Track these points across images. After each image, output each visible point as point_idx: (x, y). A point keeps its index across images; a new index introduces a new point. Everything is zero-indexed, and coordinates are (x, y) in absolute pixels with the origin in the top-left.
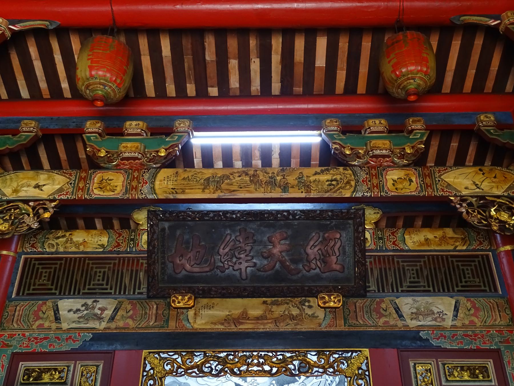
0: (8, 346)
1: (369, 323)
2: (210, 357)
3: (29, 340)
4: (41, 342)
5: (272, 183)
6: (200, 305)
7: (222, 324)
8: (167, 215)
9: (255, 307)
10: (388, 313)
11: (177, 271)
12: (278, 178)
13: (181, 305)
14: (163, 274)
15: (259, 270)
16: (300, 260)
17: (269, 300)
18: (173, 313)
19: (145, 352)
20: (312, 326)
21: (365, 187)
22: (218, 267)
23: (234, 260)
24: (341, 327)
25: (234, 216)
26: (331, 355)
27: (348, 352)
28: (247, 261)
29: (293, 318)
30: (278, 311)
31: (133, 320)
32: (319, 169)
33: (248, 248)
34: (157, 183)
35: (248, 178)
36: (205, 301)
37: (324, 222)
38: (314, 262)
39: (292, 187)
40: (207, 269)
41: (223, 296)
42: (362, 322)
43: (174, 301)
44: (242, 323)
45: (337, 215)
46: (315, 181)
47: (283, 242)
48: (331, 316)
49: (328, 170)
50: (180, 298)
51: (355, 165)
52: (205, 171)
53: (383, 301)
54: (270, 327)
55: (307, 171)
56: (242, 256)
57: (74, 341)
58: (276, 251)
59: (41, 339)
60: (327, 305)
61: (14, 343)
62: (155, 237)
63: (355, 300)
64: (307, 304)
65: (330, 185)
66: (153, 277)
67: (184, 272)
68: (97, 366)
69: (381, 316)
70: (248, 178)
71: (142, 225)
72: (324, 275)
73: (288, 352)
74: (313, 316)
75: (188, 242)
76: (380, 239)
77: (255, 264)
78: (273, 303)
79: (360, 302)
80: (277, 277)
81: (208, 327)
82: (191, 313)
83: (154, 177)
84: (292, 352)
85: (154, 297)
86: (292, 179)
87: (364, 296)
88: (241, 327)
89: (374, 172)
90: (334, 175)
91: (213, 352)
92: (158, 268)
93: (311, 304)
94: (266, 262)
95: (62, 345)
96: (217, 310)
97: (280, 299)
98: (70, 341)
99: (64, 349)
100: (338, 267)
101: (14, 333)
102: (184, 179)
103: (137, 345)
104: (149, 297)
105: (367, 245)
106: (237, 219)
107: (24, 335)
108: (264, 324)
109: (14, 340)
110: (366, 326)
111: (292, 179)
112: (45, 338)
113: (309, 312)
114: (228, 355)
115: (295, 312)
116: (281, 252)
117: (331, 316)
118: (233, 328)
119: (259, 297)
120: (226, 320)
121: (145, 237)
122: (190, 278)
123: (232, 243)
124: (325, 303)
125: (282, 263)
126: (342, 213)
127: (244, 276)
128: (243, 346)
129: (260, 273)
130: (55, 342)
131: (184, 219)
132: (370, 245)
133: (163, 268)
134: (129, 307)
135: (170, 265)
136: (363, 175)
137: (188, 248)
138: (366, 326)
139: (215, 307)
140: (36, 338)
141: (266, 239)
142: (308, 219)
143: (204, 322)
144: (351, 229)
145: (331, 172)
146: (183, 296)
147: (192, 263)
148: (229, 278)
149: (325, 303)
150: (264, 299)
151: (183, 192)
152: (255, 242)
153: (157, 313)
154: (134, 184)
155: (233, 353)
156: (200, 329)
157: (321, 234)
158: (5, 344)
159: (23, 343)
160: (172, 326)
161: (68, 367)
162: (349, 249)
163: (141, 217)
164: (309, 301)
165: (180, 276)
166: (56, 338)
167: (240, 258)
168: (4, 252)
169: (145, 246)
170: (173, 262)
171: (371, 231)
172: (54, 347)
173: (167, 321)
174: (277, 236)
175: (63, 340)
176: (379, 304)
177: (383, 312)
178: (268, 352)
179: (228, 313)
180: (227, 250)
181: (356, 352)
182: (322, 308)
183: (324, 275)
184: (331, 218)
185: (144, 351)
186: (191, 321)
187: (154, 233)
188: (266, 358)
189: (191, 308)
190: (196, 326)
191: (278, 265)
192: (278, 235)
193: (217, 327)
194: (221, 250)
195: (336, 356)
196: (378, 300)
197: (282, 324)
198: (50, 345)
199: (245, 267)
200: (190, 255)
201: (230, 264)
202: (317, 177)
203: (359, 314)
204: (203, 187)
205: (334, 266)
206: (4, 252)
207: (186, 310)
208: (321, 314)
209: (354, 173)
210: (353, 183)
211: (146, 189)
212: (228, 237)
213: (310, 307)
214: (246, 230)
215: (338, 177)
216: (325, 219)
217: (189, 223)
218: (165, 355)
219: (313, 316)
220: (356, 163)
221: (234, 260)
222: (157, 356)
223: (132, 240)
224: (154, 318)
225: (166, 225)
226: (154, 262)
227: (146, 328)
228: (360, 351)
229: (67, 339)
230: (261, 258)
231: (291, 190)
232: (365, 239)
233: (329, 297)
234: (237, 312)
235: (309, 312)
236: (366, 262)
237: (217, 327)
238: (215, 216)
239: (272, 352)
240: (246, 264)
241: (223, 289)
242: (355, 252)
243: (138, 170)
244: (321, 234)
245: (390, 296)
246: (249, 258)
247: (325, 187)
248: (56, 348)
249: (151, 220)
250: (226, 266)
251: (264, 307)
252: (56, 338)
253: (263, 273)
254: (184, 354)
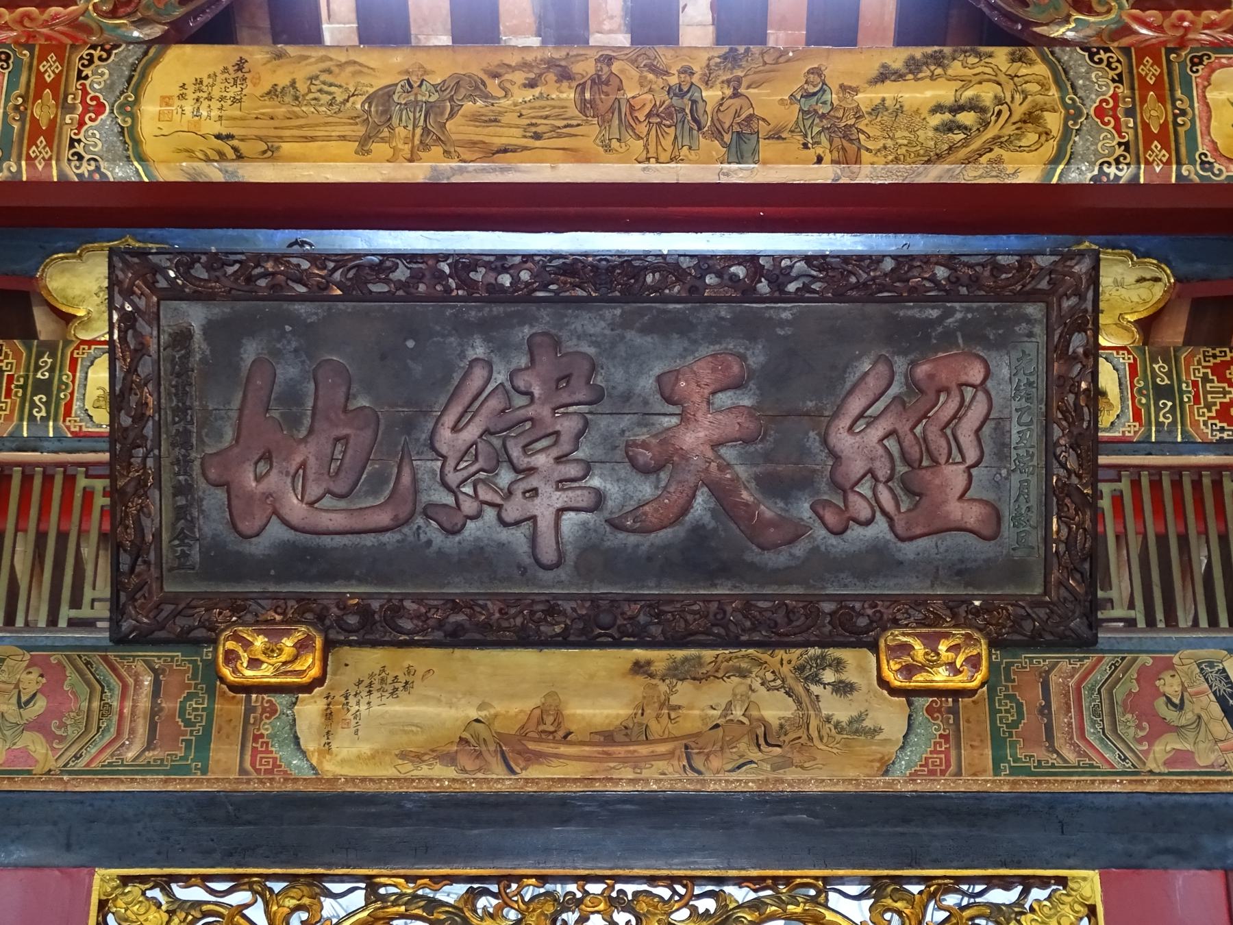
1: (1102, 760)
2: (395, 903)
5: (680, 116)
6: (347, 678)
7: (450, 759)
8: (200, 272)
9: (595, 687)
10: (1188, 717)
11: (246, 526)
12: (711, 95)
13: (265, 674)
14: (181, 536)
15: (615, 524)
16: (805, 482)
17: (660, 657)
18: (230, 709)
19: (103, 879)
20: (852, 773)
21: (1107, 141)
22: (429, 512)
23: (505, 477)
24: (978, 774)
25: (506, 280)
26: (932, 896)
27: (1006, 883)
28: (562, 484)
29: (765, 736)
30: (700, 704)
31: (50, 737)
32: (897, 58)
33: (568, 426)
34: (149, 109)
35: (568, 95)
36: (370, 659)
37: (911, 311)
38: (865, 489)
39: (776, 136)
40: (384, 518)
41: (455, 639)
42: (1071, 757)
43: (231, 657)
44: (538, 757)
45: (975, 281)
46: (876, 110)
47: (724, 399)
48: (937, 728)
49: (938, 60)
50: (260, 642)
51: (1064, 42)
52: (372, 58)
53: (1170, 666)
54: (662, 776)
55: (841, 66)
56: (541, 460)
58: (693, 439)
60: (919, 680)
62: (145, 368)
63: (1042, 660)
64: (829, 676)
65: (949, 128)
66: (138, 551)
67: (276, 531)
69: (1161, 728)
70: (568, 95)
71: (86, 322)
72: (909, 550)
73: (740, 882)
74: (857, 729)
75: (292, 397)
76: (1163, 392)
77: (599, 499)
78: (676, 672)
79: (1065, 669)
80: (699, 555)
81: (388, 774)
82: (310, 709)
83: (136, 79)
84: (757, 883)
85: (144, 639)
86: (772, 101)
87: (1087, 643)
88: (535, 772)
89: (1149, 71)
90: (966, 83)
91: (408, 879)
92: (159, 510)
93: (850, 676)
94: (645, 489)
96: (425, 699)
97: (708, 654)
100: (972, 514)
102: (273, 93)
103: (68, 847)
104: (120, 640)
105: (1105, 419)
106: (521, 296)
108: (636, 762)
110: (1092, 771)
111: (772, 101)
113: (840, 710)
114: (472, 895)
115: (776, 709)
116: (716, 445)
117: (937, 728)
118: (497, 780)
119: (617, 644)
120: (466, 744)
121: (99, 376)
122: (303, 557)
123: (495, 404)
124: (909, 671)
125: (722, 493)
126: (997, 269)
127: (548, 553)
128: (546, 852)
129: (621, 535)
131: (277, 293)
132: (1115, 419)
133: (181, 513)
134: (32, 681)
135: (214, 499)
136: (1099, 86)
137: (293, 421)
138: (1092, 771)
139: (419, 688)
141: (647, 384)
142: (839, 297)
143: (366, 748)
144: (1035, 346)
145: (956, 68)
146: (275, 634)
147: (314, 491)
148: (480, 559)
149: (909, 671)
150: (640, 653)
151: (270, 153)
152: (598, 397)
153: (155, 711)
154: (43, 112)
155: (494, 888)
156: (352, 780)
157: (900, 364)
160: (225, 769)
162: (1023, 435)
163: (80, 284)
164: (838, 665)
165: (258, 547)
167: (531, 470)
169: (102, 417)
170: (226, 485)
171: (1124, 360)
173: (203, 743)
174: (699, 370)
176: (1148, 677)
177: (1170, 715)
178: (652, 880)
179: (474, 714)
180: (471, 433)
181: (1044, 882)
182: (894, 692)
183: (909, 550)
184: (948, 293)
185: (100, 872)
186: (310, 744)
187: (141, 350)
188: (643, 907)
189: (308, 688)
190: (330, 768)
191: (701, 505)
192: (705, 373)
193: (424, 771)
194: (445, 433)
195: (951, 900)
196: (1146, 659)
197: (715, 763)
199: (553, 510)
200: (308, 452)
201: (485, 495)
202: (888, 92)
203: (1061, 721)
204: (361, 130)
205: (956, 511)
207: (281, 700)
208: (890, 718)
209: (1062, 76)
210: (1053, 121)
211: (97, 135)
212: (479, 374)
213: (842, 688)
214: (557, 344)
215: (987, 93)
216: (917, 296)
217: (301, 308)
218: (196, 893)
219: (857, 729)
220: (1065, 31)
221: (505, 477)
222: (156, 893)
223: (43, 387)
224: (142, 729)
225: (196, 316)
226: (141, 483)
227: (109, 771)
228: (1063, 881)
230: (624, 470)
231: (767, 148)
232: (1096, 394)
233: (931, 642)
234: (514, 709)
235: (840, 710)
236: (1097, 495)
237: (424, 771)
238: (417, 277)
239: (671, 881)
240: (559, 499)
241: (454, 605)
242: (1050, 449)
243: (59, 50)
244: (900, 364)
245: (1201, 644)
246: (572, 470)
247: (926, 136)
249: (128, 294)
250: (469, 507)
251: (637, 686)
253: (633, 539)
254: (277, 886)
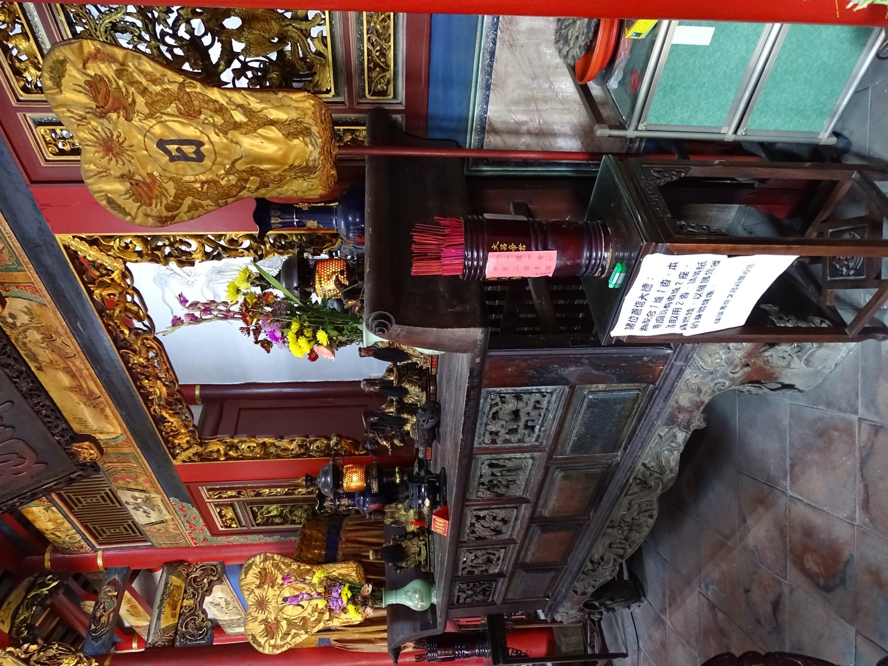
7: (103, 410)
20: (51, 314)
30: (45, 355)
44: (92, 393)
115: (34, 336)
118: (105, 398)
139: (80, 416)
156: (120, 425)
168: (100, 562)
179: (83, 405)
190: (119, 431)
206: (100, 562)
234: (75, 398)
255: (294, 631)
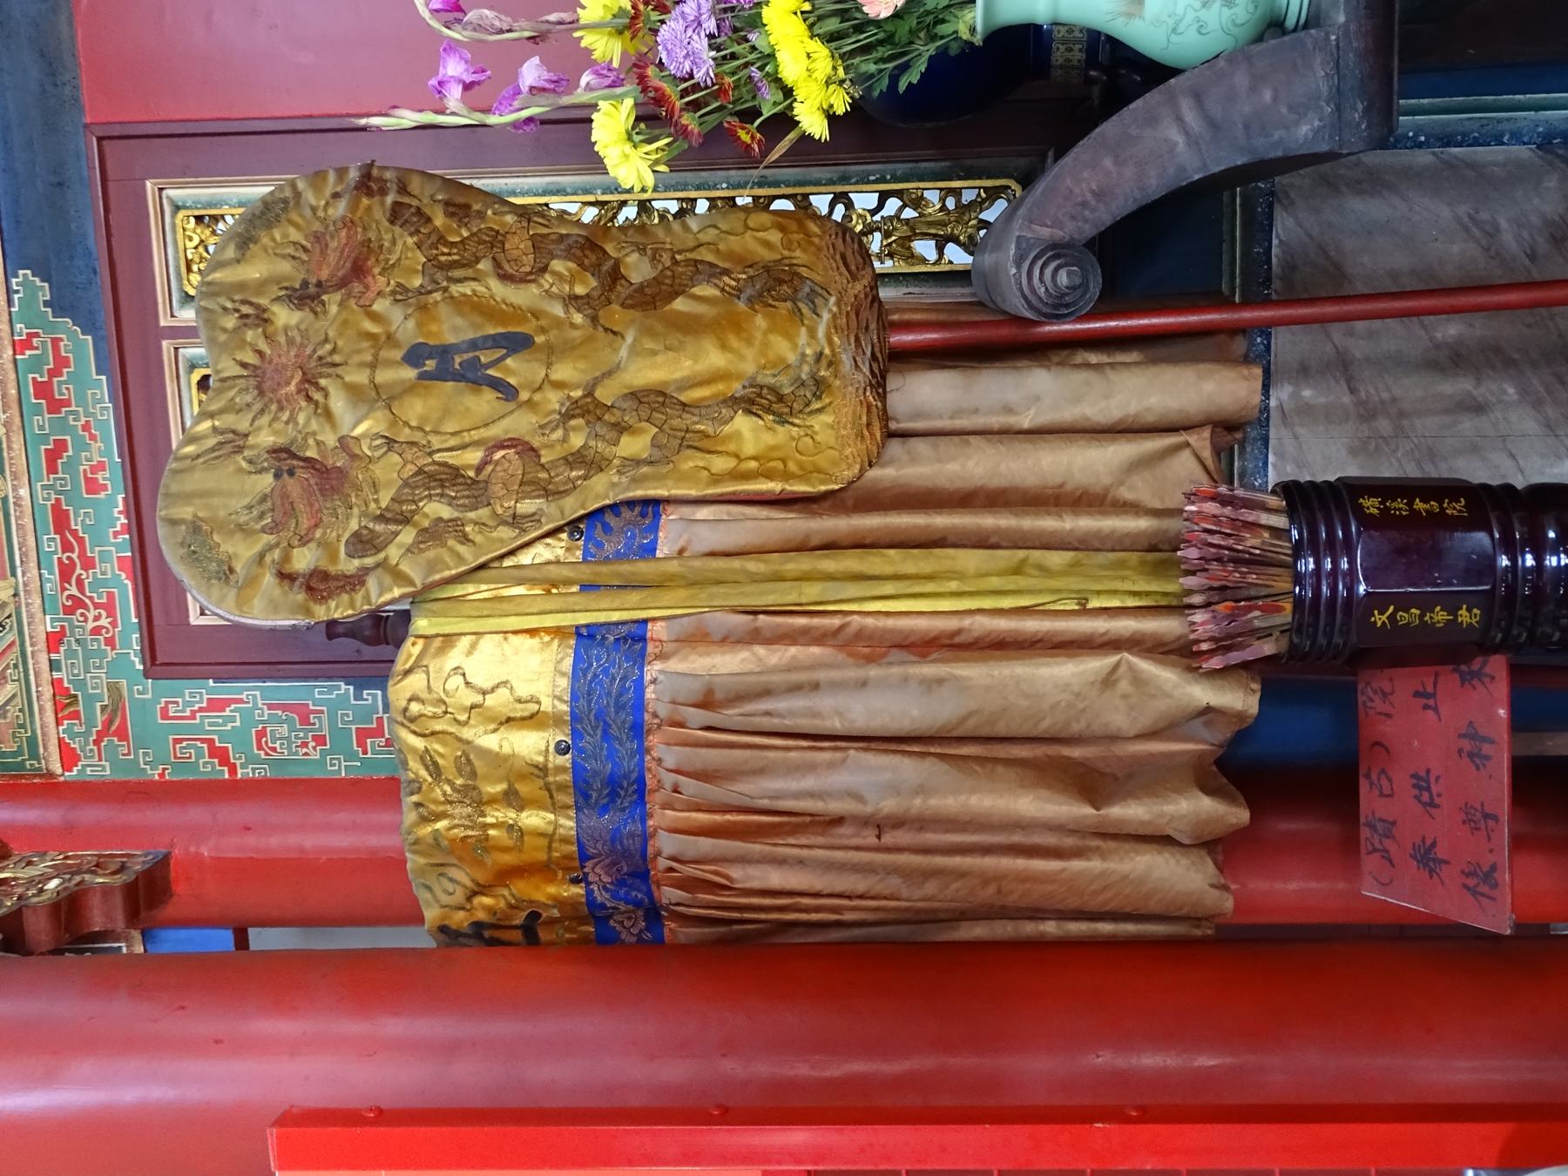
0: (115, 709)
3: (78, 603)
4: (81, 541)
57: (61, 362)
59: (67, 547)
61: (97, 682)
68: (177, 208)
95: (86, 427)
98: (63, 388)
99: (105, 412)
101: (47, 691)
107: (54, 641)
109: (81, 684)
112: (61, 521)
130: (71, 466)
140: (66, 572)
158: (108, 723)
159: (96, 631)
161: (192, 367)
166: (52, 469)
172: (101, 466)
175: (63, 426)
198: (93, 486)
229: (55, 406)
248: (105, 450)
252: (52, 469)
255: (437, 509)
